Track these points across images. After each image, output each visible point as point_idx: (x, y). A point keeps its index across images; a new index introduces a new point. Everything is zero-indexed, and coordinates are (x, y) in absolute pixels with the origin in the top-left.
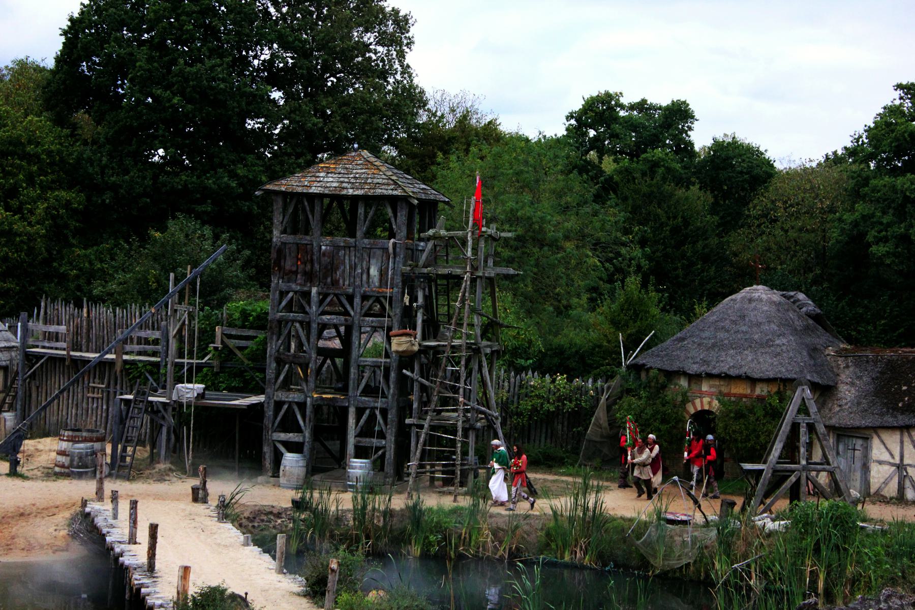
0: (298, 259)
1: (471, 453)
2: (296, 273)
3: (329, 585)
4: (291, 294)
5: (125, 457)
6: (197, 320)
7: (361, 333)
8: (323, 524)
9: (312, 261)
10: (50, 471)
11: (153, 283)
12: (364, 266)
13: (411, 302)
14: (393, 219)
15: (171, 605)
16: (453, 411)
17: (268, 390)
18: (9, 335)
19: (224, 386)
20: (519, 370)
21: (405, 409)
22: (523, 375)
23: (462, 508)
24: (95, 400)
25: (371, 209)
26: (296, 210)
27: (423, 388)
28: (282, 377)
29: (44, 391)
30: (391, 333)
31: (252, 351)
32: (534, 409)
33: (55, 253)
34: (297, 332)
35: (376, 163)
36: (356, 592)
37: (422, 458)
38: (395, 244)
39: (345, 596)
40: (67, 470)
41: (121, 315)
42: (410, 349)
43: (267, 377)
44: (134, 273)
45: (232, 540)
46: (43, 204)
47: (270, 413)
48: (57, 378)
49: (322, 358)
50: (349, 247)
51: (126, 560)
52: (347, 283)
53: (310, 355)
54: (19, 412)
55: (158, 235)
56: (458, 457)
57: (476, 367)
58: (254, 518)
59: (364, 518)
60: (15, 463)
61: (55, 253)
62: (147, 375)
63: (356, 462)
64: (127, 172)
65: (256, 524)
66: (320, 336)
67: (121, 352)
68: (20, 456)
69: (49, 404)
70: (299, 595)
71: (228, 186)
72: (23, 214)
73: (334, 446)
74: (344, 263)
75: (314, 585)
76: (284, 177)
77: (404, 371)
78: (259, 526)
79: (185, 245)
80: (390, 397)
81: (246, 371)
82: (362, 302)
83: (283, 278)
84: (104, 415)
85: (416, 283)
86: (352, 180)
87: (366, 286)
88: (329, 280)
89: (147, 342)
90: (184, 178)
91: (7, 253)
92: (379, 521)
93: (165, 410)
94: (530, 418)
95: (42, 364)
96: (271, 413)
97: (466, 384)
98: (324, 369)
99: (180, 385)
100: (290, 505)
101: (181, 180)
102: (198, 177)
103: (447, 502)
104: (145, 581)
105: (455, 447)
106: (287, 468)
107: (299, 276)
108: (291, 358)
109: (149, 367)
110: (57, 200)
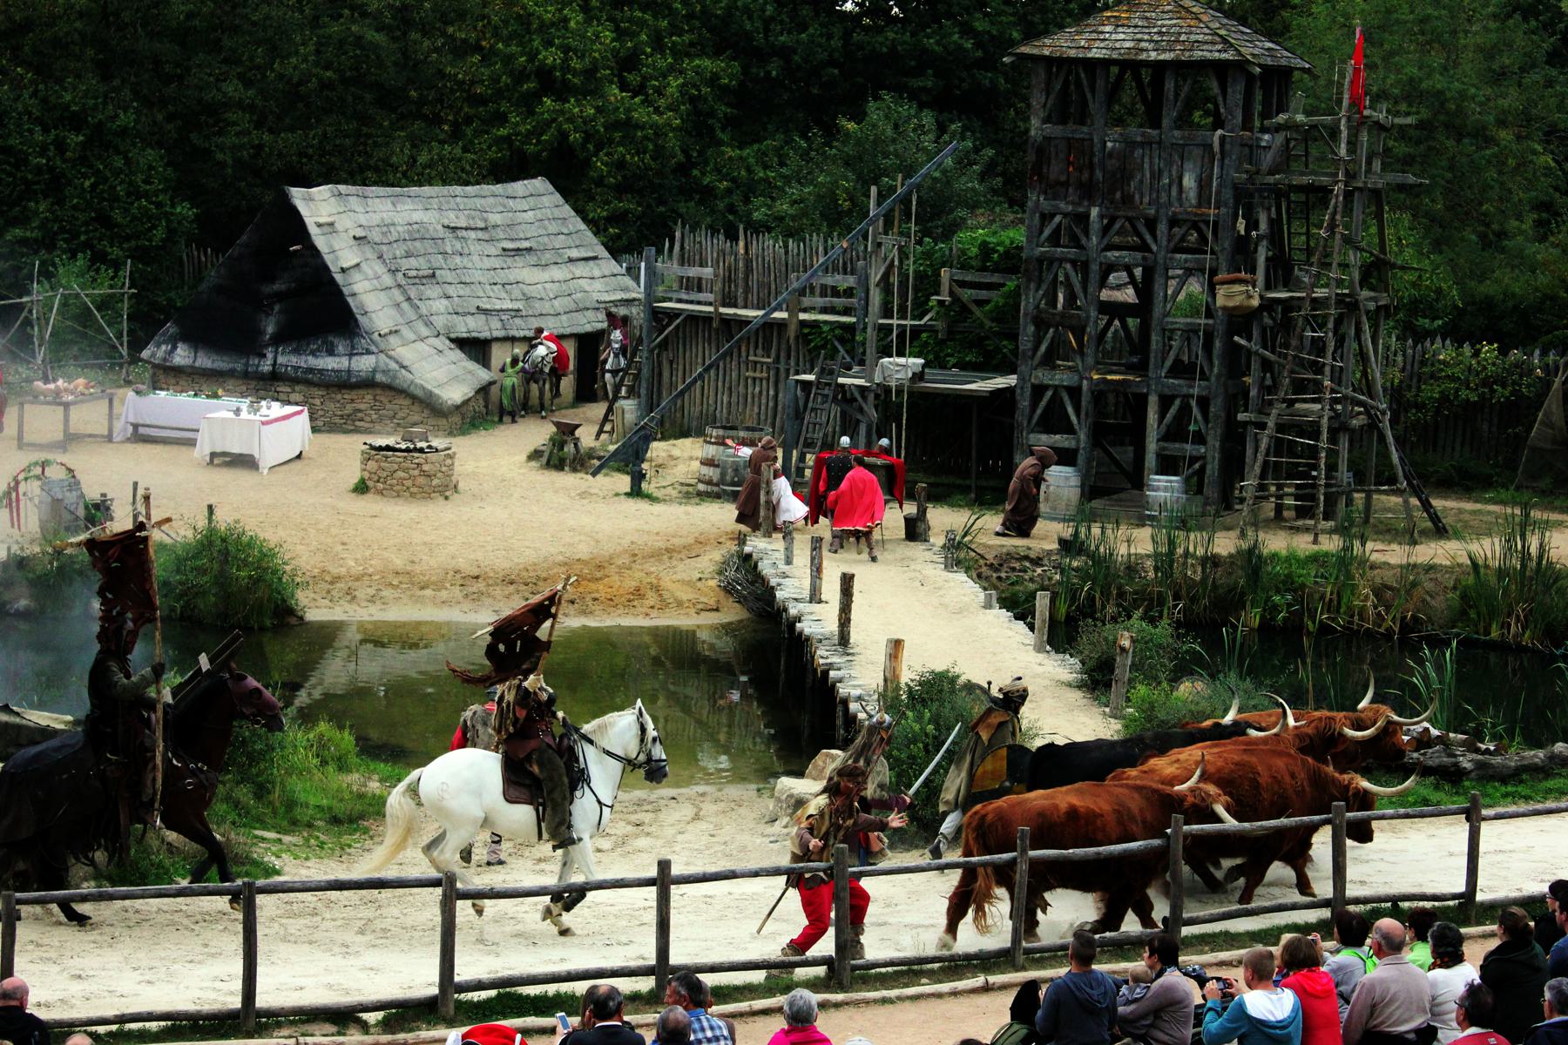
0: (1069, 163)
1: (1343, 466)
2: (1066, 184)
3: (1117, 671)
4: (1058, 219)
5: (804, 469)
6: (912, 259)
7: (1168, 278)
8: (1106, 576)
9: (1091, 166)
10: (691, 489)
11: (845, 200)
12: (1174, 173)
13: (1247, 229)
14: (1220, 99)
15: (876, 697)
16: (1314, 401)
17: (1022, 368)
18: (628, 281)
19: (952, 360)
20: (1421, 336)
21: (1238, 398)
22: (1428, 343)
23: (1326, 554)
24: (758, 382)
25: (1185, 81)
26: (1066, 84)
27: (1266, 365)
28: (1043, 348)
29: (681, 367)
30: (1216, 278)
31: (997, 307)
32: (1444, 397)
33: (695, 154)
34: (1067, 276)
35: (1194, 10)
36: (1159, 683)
37: (1263, 476)
38: (1223, 139)
39: (1142, 690)
40: (716, 489)
41: (796, 251)
42: (1246, 303)
43: (1021, 348)
44: (815, 186)
45: (966, 599)
46: (676, 79)
47: (1024, 403)
48: (700, 348)
49: (1106, 318)
50: (1151, 143)
51: (806, 627)
52: (1146, 200)
53: (1087, 312)
54: (643, 399)
55: (851, 126)
56: (1320, 474)
57: (1353, 332)
58: (1001, 565)
59: (1171, 567)
60: (638, 478)
61: (695, 154)
62: (836, 343)
63: (1159, 481)
64: (803, 27)
65: (1003, 575)
66: (1103, 283)
67: (794, 309)
68: (645, 466)
69: (688, 387)
70: (1069, 685)
71: (960, 48)
72: (647, 95)
73: (1125, 454)
74: (1141, 168)
75: (1093, 670)
76: (1046, 33)
77: (1236, 338)
78: (1008, 578)
79: (894, 141)
80: (1213, 379)
81: (987, 338)
82: (1170, 229)
83: (1045, 193)
84: (771, 404)
85: (1256, 200)
86: (1156, 38)
87: (1177, 204)
88: (1118, 195)
89: (835, 292)
90: (891, 35)
91: (624, 156)
92: (1195, 572)
93: (864, 398)
94: (1438, 411)
95: (677, 327)
96: (1026, 403)
97: (1334, 359)
98: (1110, 334)
99: (886, 360)
100: (1055, 546)
101: (887, 39)
102: (913, 35)
103: (1303, 544)
104: (835, 659)
105: (1317, 458)
106: (1052, 488)
107: (1071, 190)
108: (1058, 318)
109: (838, 332)
110: (697, 73)
